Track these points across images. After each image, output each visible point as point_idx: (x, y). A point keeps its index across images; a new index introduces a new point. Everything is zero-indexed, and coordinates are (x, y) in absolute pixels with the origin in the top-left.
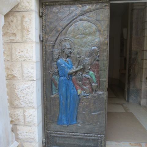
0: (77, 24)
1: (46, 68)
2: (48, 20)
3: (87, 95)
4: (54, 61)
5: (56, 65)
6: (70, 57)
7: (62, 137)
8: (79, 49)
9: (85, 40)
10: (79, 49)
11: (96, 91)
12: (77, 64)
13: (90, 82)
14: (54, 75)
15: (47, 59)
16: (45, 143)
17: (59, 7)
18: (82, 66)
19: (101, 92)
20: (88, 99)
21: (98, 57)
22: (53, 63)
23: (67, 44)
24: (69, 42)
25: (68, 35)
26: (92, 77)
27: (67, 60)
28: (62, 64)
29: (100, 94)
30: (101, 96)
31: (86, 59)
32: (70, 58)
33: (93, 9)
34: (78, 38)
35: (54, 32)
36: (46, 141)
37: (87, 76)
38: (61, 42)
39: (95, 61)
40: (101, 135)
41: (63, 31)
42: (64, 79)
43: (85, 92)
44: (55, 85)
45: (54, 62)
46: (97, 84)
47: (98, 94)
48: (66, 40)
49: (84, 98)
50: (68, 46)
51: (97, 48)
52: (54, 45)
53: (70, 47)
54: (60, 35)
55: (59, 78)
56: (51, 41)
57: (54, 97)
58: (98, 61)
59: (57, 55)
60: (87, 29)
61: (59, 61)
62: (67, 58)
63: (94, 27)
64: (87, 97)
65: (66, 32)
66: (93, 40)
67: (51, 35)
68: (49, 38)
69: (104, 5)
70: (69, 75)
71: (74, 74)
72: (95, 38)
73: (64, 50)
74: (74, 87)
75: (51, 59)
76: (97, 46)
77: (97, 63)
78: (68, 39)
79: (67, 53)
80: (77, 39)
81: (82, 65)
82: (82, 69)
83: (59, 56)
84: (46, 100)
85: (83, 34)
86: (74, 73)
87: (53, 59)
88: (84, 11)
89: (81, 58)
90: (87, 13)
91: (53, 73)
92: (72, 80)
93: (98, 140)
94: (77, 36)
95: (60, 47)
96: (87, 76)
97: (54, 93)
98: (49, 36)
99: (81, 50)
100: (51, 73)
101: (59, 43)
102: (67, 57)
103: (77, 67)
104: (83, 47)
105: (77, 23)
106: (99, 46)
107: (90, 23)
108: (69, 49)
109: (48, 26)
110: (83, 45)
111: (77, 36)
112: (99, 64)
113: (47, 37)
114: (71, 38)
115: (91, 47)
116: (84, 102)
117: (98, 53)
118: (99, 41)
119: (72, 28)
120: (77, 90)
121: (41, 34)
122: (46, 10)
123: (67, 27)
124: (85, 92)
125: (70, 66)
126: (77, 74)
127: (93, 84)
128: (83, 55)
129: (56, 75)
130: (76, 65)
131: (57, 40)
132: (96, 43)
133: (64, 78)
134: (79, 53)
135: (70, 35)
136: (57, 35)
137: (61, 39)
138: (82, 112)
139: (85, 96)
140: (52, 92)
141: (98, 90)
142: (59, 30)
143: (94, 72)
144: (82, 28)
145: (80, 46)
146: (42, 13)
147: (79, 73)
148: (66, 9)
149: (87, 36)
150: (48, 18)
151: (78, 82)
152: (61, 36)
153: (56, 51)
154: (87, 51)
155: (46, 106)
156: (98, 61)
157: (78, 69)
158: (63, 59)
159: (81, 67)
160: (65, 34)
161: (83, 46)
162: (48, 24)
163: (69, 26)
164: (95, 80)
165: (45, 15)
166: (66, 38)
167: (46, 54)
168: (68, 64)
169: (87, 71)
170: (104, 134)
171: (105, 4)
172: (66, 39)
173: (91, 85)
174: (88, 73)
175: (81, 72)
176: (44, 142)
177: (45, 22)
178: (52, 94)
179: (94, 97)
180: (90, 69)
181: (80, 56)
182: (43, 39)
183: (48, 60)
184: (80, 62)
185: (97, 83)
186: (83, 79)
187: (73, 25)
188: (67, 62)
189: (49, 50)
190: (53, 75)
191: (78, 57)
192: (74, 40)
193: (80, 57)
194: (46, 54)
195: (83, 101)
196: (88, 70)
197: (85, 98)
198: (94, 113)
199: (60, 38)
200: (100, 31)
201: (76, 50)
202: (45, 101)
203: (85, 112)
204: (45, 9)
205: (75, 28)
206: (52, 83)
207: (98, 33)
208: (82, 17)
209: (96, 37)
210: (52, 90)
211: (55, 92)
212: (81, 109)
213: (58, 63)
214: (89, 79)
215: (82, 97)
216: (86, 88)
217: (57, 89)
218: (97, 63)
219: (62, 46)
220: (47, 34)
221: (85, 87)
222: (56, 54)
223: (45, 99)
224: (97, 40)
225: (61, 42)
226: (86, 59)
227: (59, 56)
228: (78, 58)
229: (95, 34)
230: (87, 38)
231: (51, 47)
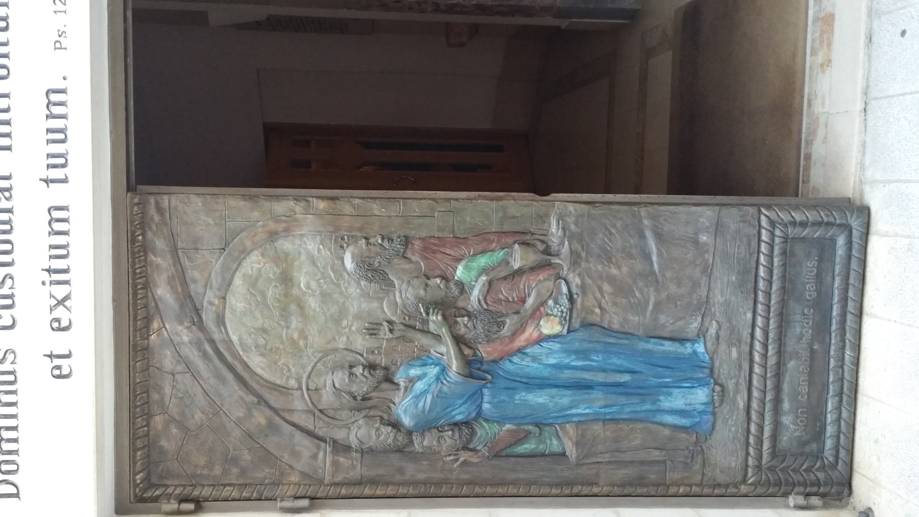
0: (240, 339)
1: (439, 484)
2: (217, 470)
3: (565, 289)
4: (406, 445)
5: (427, 434)
8: (354, 328)
9: (313, 303)
10: (354, 328)
11: (547, 252)
12: (419, 336)
13: (505, 278)
14: (471, 446)
15: (398, 478)
16: (807, 495)
17: (158, 421)
18: (433, 318)
19: (554, 229)
20: (583, 288)
21: (391, 240)
22: (417, 447)
23: (329, 382)
24: (319, 375)
25: (288, 379)
26: (484, 271)
27: (402, 384)
28: (421, 404)
29: (564, 229)
30: (573, 227)
31: (397, 295)
32: (393, 368)
33: (174, 265)
34: (303, 335)
35: (271, 443)
36: (798, 494)
37: (476, 293)
38: (320, 411)
39: (409, 255)
41: (272, 403)
42: (493, 396)
43: (551, 302)
44: (519, 442)
45: (412, 442)
46: (516, 246)
47: (562, 243)
48: (312, 387)
49: (582, 304)
50: (340, 378)
51: (351, 248)
52: (335, 442)
53: (342, 368)
54: (287, 416)
55: (487, 420)
56: (315, 457)
57: (577, 444)
58: (407, 241)
59: (378, 429)
60: (263, 295)
61: (407, 421)
63: (254, 263)
64: (574, 290)
65: (274, 387)
66: (313, 263)
67: (286, 457)
68: (299, 466)
69: (157, 218)
70: (471, 376)
71: (467, 351)
72: (303, 257)
73: (355, 398)
74: (528, 351)
75: (395, 458)
76: (342, 247)
77: (417, 244)
78: (305, 376)
79: (372, 381)
80: (306, 338)
81: (428, 314)
82: (445, 317)
83: (382, 418)
84: (591, 484)
85: (285, 314)
86: (460, 350)
87: (400, 451)
88: (182, 306)
89: (394, 319)
90: (190, 296)
91: (465, 448)
92: (495, 361)
93: (785, 239)
94: (296, 336)
95: (344, 414)
96: (476, 293)
97: (554, 445)
98: (291, 467)
99: (358, 317)
100: (462, 459)
101: (326, 419)
102: (385, 386)
103: (438, 338)
104: (342, 312)
105: (235, 338)
106: (343, 239)
107: (238, 281)
108: (351, 374)
109: (243, 472)
110: (334, 309)
111: (296, 336)
112: (423, 235)
113: (294, 478)
114: (303, 367)
115: (347, 276)
116: (600, 307)
117: (372, 240)
118: (318, 238)
119: (256, 362)
120: (542, 339)
121: (279, 505)
122: (169, 483)
123: (254, 385)
124: (551, 302)
125: (433, 371)
126: (469, 336)
127: (516, 265)
128: (382, 308)
129: (473, 433)
130: (425, 340)
131: (311, 427)
132: (326, 253)
133: (486, 399)
134: (373, 330)
135: (289, 370)
136: (287, 428)
137: (307, 411)
138: (648, 314)
139: (571, 299)
140: (552, 455)
141: (543, 242)
142: (263, 421)
143: (458, 260)
144: (258, 314)
145: (337, 321)
146: (183, 500)
147: (465, 325)
148: (168, 390)
149: (295, 292)
150: (205, 472)
151: (506, 331)
152: (291, 411)
153: (362, 433)
154: (362, 289)
155: (623, 485)
156: (407, 241)
157: (444, 331)
158: (397, 400)
159: (435, 319)
160: (283, 390)
161: (340, 312)
162: (235, 470)
163: (245, 375)
164: (500, 254)
165: (194, 486)
166: (300, 388)
167: (373, 482)
168: (419, 378)
169: (455, 291)
170: (760, 212)
171: (152, 211)
172: (308, 389)
173: (520, 272)
174: (462, 287)
175: (459, 319)
176: (801, 500)
177: (225, 485)
178: (564, 454)
179: (575, 259)
180: (445, 278)
181: (385, 324)
182: (304, 497)
183: (401, 471)
184: (412, 322)
185: (510, 247)
186: (491, 308)
187: (245, 359)
188: (412, 381)
189: (353, 467)
190: (474, 450)
191: (391, 331)
192: (310, 351)
193: (390, 322)
194: (373, 482)
195: (597, 310)
196: (452, 285)
197: (579, 301)
198: (655, 258)
199: (304, 416)
200: (273, 236)
201: (360, 343)
202: (596, 490)
203: (647, 302)
204: (167, 486)
205: (257, 346)
206: (508, 456)
207: (285, 245)
208: (208, 318)
209: (300, 253)
210: (543, 455)
211: (555, 442)
212: (637, 319)
213: (416, 425)
214: (490, 283)
215: (574, 315)
216: (533, 294)
217: (537, 430)
218: (417, 244)
219: (336, 405)
220: (282, 474)
221: (530, 301)
222: (374, 437)
223: (586, 490)
224: (312, 246)
225: (320, 411)
226: (397, 295)
227: (382, 418)
228: (397, 334)
229: (287, 255)
230: (304, 293)
231: (341, 459)
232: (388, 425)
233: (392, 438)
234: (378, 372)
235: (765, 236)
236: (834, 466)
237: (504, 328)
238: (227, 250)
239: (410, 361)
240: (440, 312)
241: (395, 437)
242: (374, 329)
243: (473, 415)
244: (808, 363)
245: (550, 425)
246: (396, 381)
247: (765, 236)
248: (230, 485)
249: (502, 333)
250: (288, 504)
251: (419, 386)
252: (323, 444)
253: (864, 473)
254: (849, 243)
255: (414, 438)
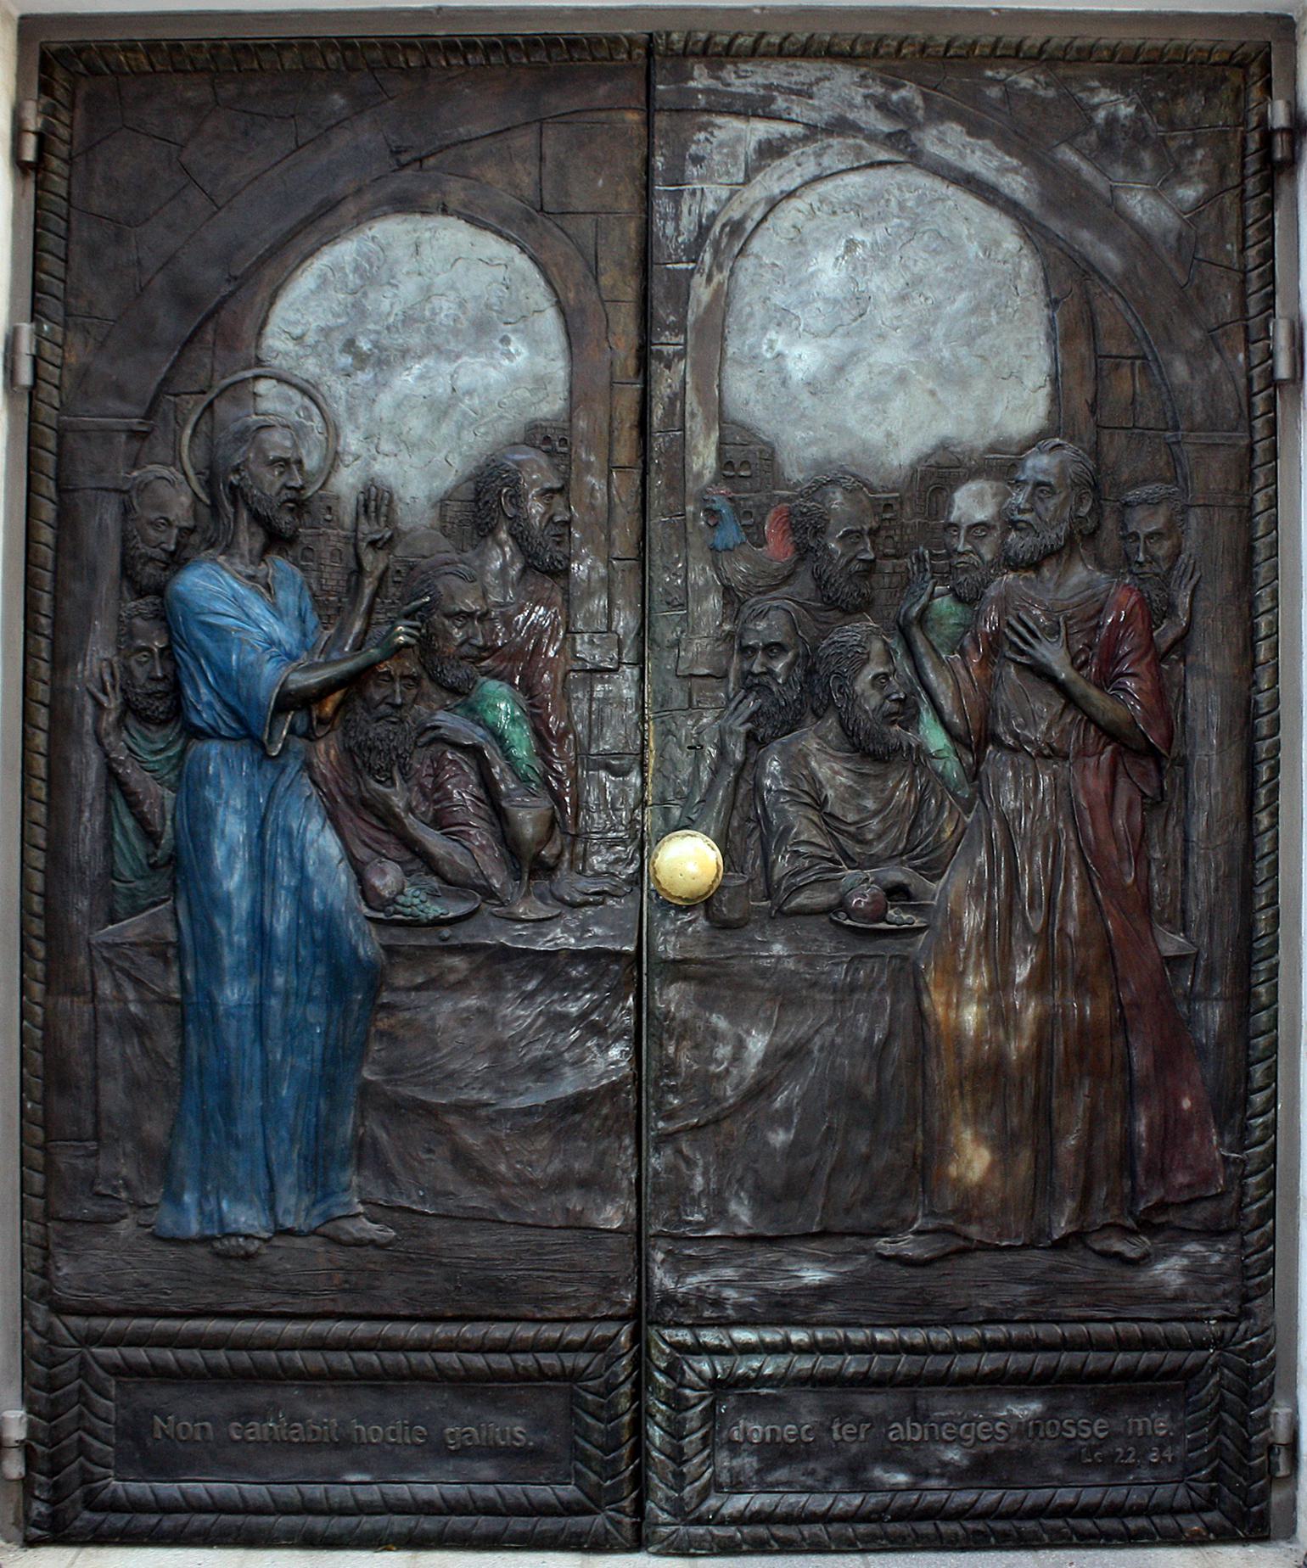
6: (292, 541)
7: (214, 1376)
36: (31, 1427)
38: (210, 405)
40: (600, 1331)
62: (266, 550)
81: (407, 616)
83: (191, 531)
84: (47, 982)
93: (574, 1376)
121: (26, 328)
122: (79, 113)
139: (438, 922)
146: (41, 137)
165: (69, 161)
201: (347, 481)
204: (71, 108)
228: (368, 558)
232: (178, 544)
233: (150, 551)
234: (288, 518)
235: (577, 1334)
236: (91, 1503)
237: (379, 782)
238: (539, 217)
239: (310, 588)
240: (413, 641)
241: (152, 559)
242: (377, 509)
243: (196, 721)
244: (310, 1438)
245: (174, 888)
246: (268, 558)
247: (577, 1334)
248: (68, 229)
249: (365, 773)
250: (26, 346)
251: (258, 609)
252: (140, 411)
253: (78, 1562)
254: (568, 1509)
255: (150, 599)
